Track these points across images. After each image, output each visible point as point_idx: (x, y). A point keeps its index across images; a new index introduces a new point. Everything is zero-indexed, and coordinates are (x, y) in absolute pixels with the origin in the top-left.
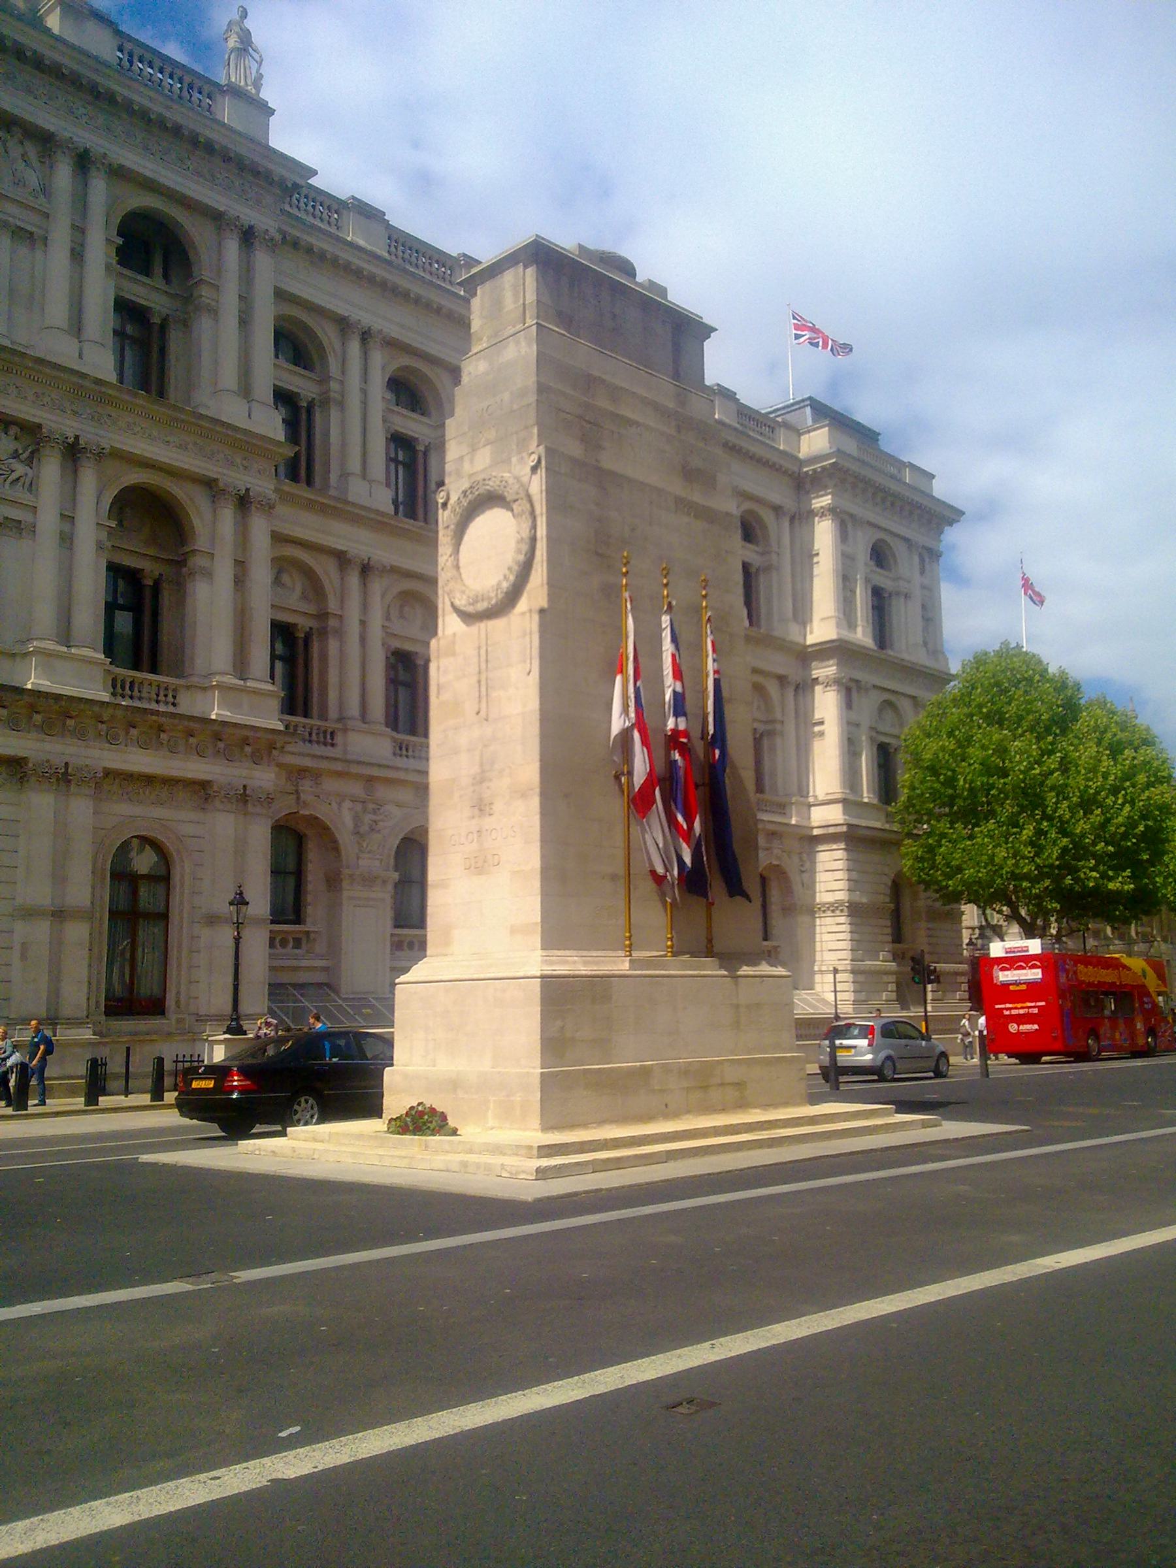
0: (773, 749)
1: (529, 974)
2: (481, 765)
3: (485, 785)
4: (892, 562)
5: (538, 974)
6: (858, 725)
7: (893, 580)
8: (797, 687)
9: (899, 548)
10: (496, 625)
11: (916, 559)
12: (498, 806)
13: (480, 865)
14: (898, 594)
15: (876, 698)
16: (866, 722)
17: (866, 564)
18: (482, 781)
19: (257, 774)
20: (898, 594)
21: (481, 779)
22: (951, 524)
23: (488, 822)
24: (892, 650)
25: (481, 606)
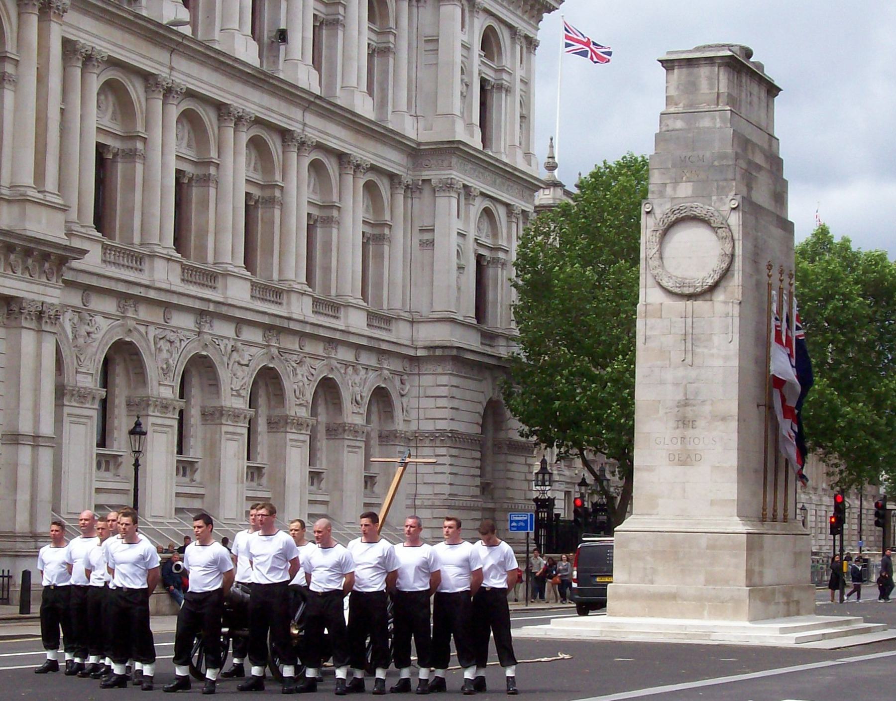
0: (380, 256)
1: (737, 531)
2: (686, 394)
3: (689, 409)
4: (495, 49)
5: (745, 531)
6: (463, 236)
7: (496, 70)
8: (407, 187)
9: (504, 35)
10: (699, 305)
11: (518, 48)
12: (701, 423)
13: (685, 458)
14: (500, 87)
15: (479, 204)
16: (472, 233)
17: (480, 56)
18: (686, 405)
19: (49, 291)
20: (500, 87)
21: (685, 403)
22: (549, 11)
23: (690, 433)
24: (491, 150)
25: (687, 291)
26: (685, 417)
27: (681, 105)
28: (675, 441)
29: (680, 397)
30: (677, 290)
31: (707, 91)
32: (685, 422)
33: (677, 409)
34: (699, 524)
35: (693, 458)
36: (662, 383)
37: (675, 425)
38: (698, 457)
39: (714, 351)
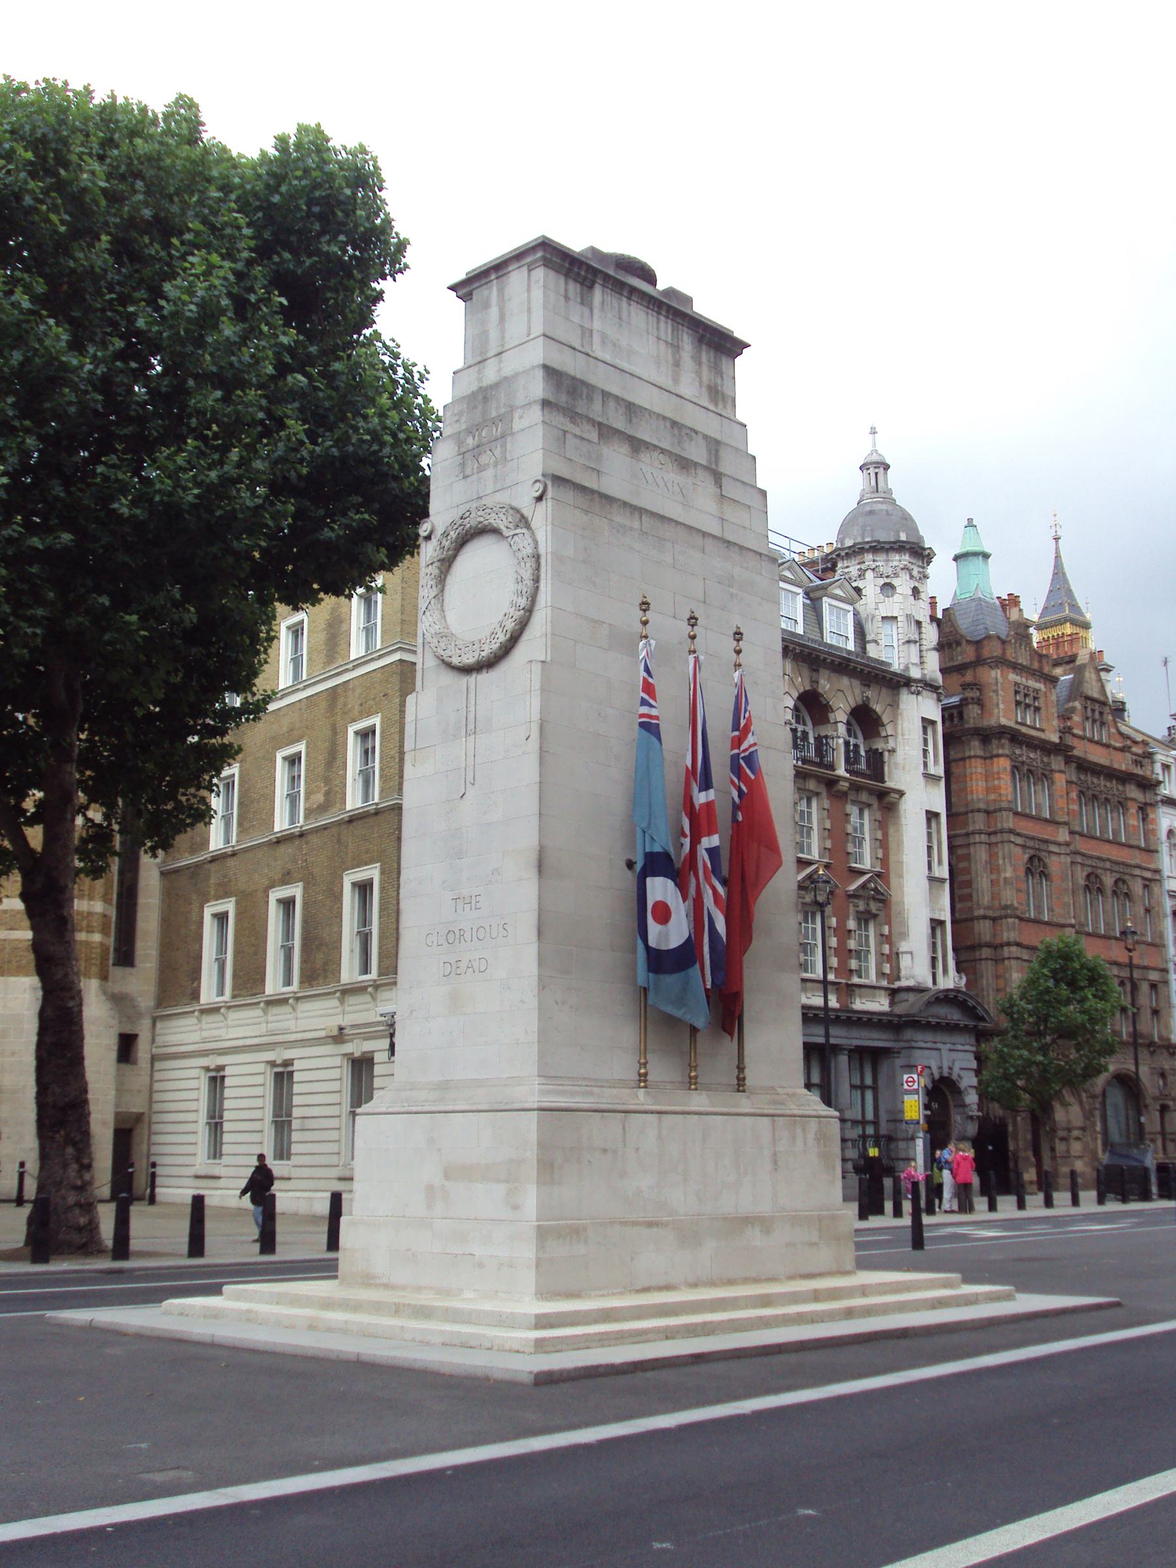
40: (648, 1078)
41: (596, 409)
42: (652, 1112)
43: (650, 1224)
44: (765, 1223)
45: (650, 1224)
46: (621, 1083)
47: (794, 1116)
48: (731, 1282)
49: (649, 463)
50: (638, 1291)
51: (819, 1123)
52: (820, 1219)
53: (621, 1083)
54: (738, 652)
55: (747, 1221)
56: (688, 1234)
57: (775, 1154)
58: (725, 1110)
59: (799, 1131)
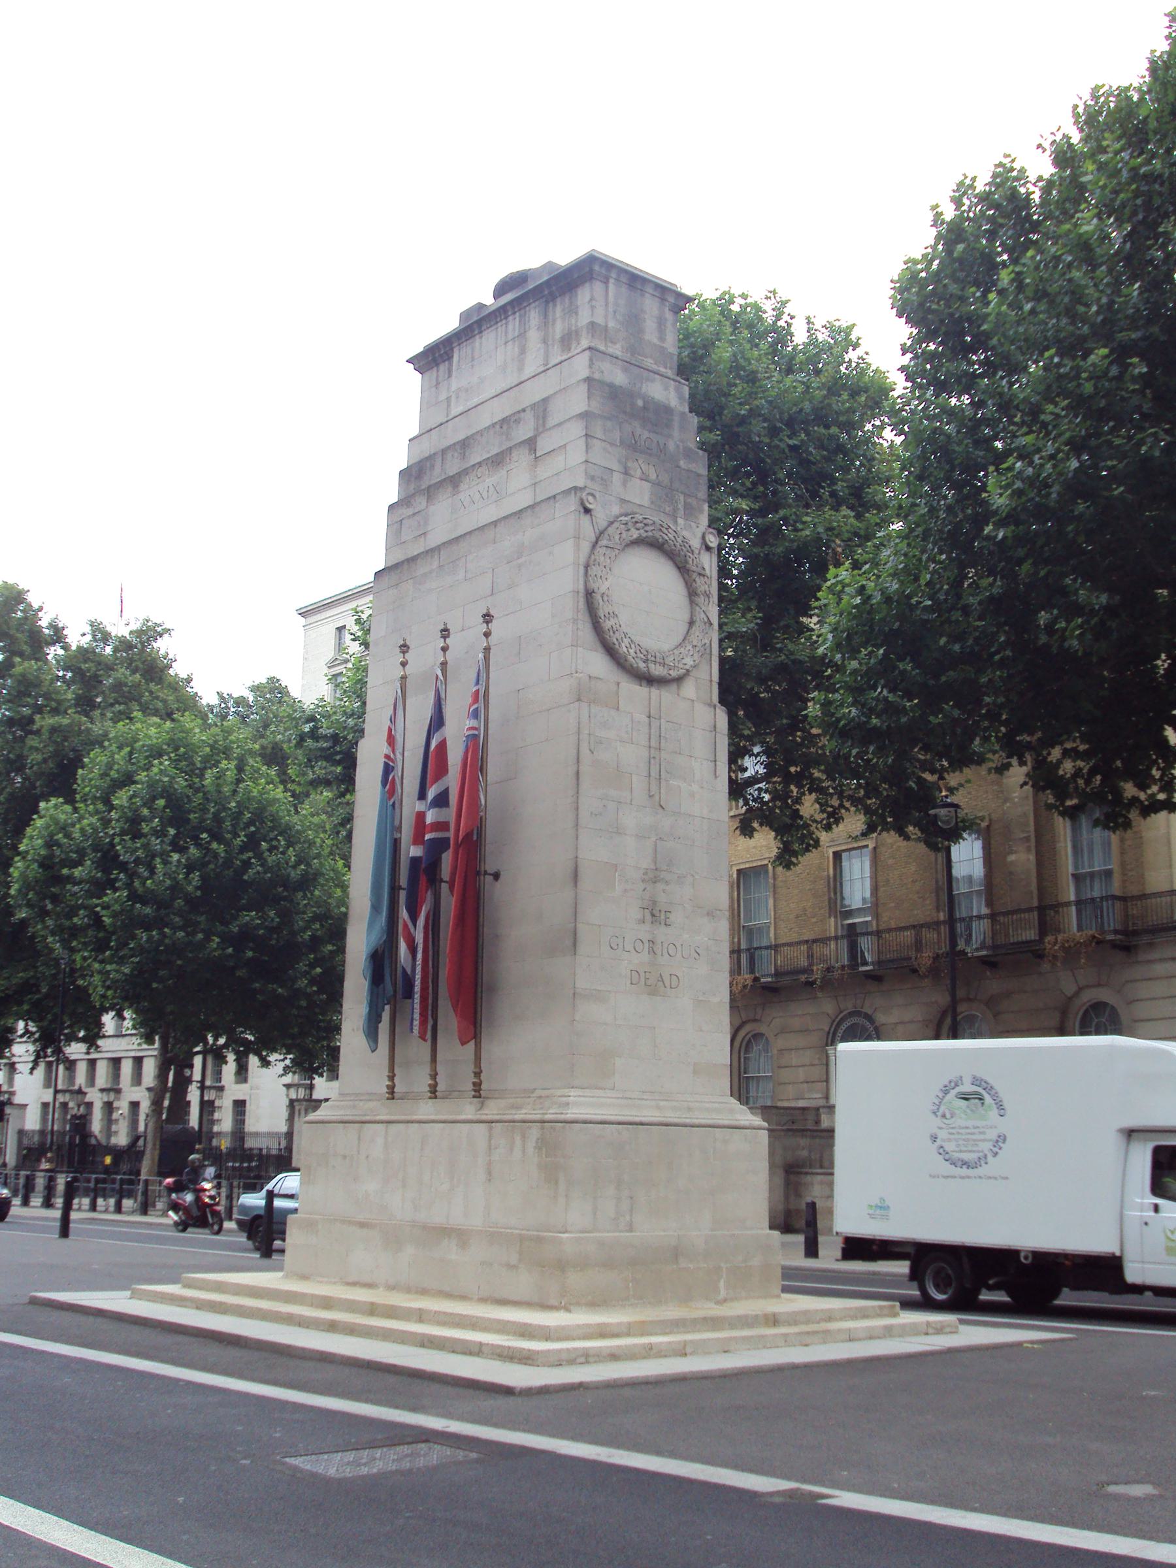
3: (660, 886)
12: (677, 917)
18: (655, 881)
21: (654, 877)
25: (657, 671)
26: (655, 903)
27: (618, 346)
28: (639, 945)
29: (647, 863)
30: (642, 665)
31: (656, 341)
32: (655, 914)
33: (643, 886)
34: (689, 1109)
35: (667, 983)
36: (618, 831)
37: (640, 916)
38: (674, 984)
39: (695, 787)
40: (483, 1087)
41: (436, 475)
42: (382, 1122)
43: (362, 1225)
44: (460, 1236)
45: (362, 1225)
46: (371, 1096)
47: (514, 1122)
48: (424, 1292)
49: (470, 490)
50: (348, 1284)
51: (543, 1128)
52: (522, 1238)
53: (371, 1096)
54: (404, 664)
55: (444, 1232)
56: (393, 1238)
57: (489, 1164)
58: (451, 1117)
59: (518, 1139)
